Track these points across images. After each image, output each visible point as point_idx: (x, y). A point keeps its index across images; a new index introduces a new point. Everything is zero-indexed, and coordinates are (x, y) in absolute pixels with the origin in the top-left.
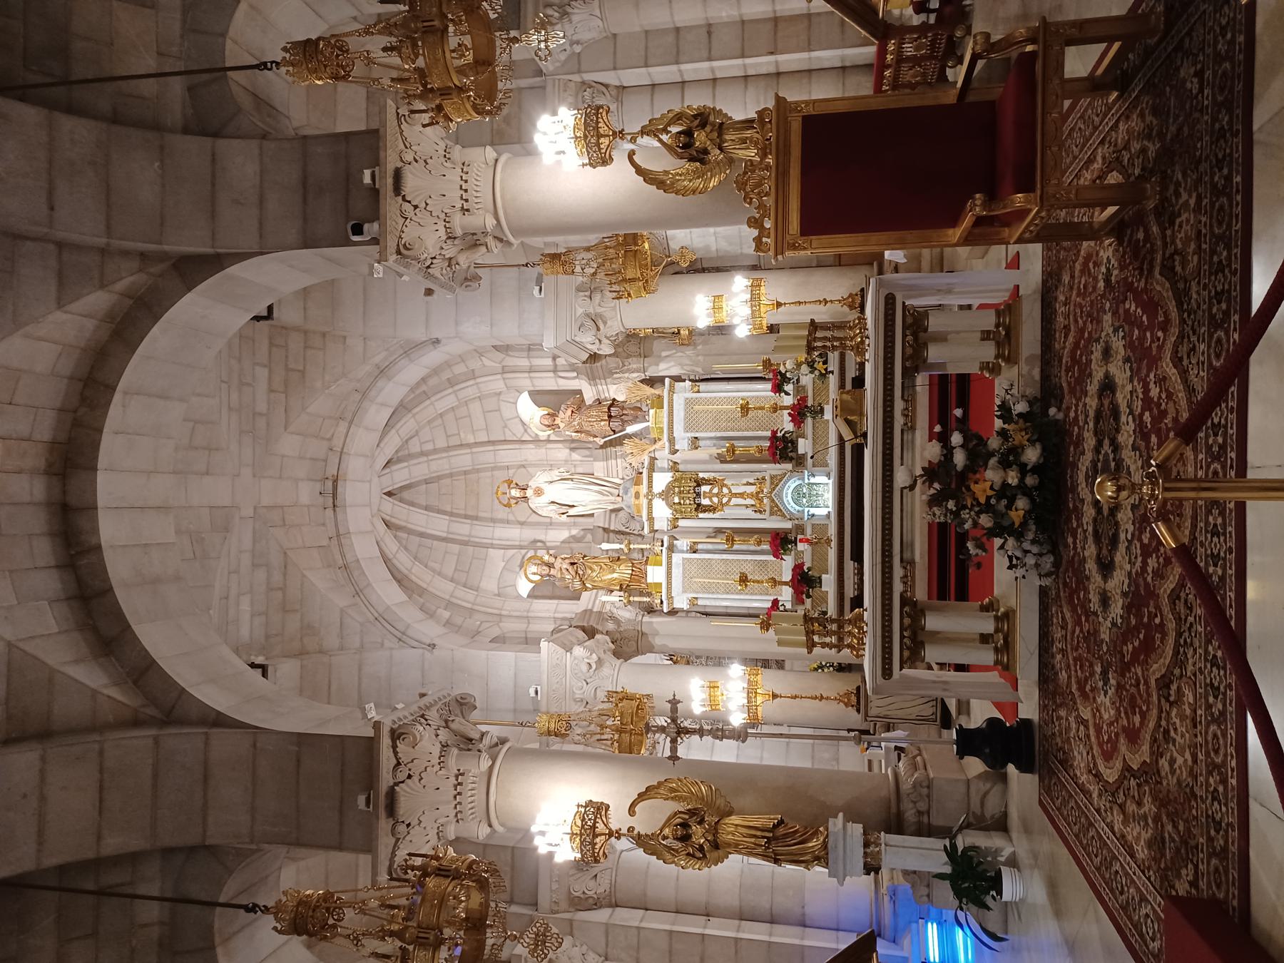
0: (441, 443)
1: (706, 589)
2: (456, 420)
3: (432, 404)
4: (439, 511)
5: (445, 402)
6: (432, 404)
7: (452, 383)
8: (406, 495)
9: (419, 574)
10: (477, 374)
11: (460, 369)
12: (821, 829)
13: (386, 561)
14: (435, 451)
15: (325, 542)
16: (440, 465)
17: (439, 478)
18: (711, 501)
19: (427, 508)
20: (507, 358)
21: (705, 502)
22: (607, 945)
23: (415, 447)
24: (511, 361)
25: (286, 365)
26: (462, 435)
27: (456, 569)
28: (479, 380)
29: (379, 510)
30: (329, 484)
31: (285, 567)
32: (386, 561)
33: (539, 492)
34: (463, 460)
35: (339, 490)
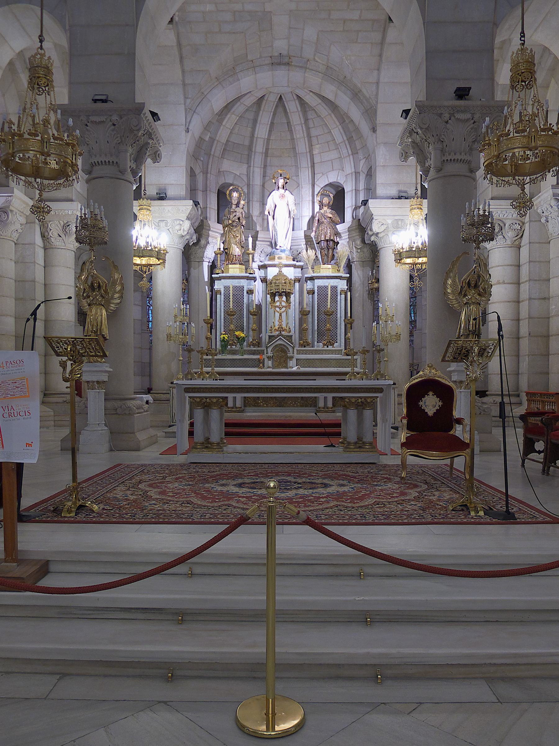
0: (313, 132)
1: (227, 297)
2: (327, 142)
3: (337, 126)
4: (270, 131)
5: (338, 134)
6: (337, 126)
7: (350, 140)
8: (280, 109)
9: (230, 120)
10: (355, 156)
11: (358, 145)
12: (104, 360)
13: (239, 99)
14: (308, 129)
15: (250, 58)
16: (299, 132)
17: (291, 131)
18: (278, 301)
19: (272, 123)
20: (364, 176)
21: (277, 298)
22: (23, 244)
23: (311, 115)
24: (362, 177)
25: (360, 31)
26: (317, 146)
27: (234, 143)
28: (351, 157)
29: (270, 92)
30: (286, 60)
31: (234, 33)
32: (239, 99)
33: (283, 196)
34: (302, 146)
35: (283, 67)
